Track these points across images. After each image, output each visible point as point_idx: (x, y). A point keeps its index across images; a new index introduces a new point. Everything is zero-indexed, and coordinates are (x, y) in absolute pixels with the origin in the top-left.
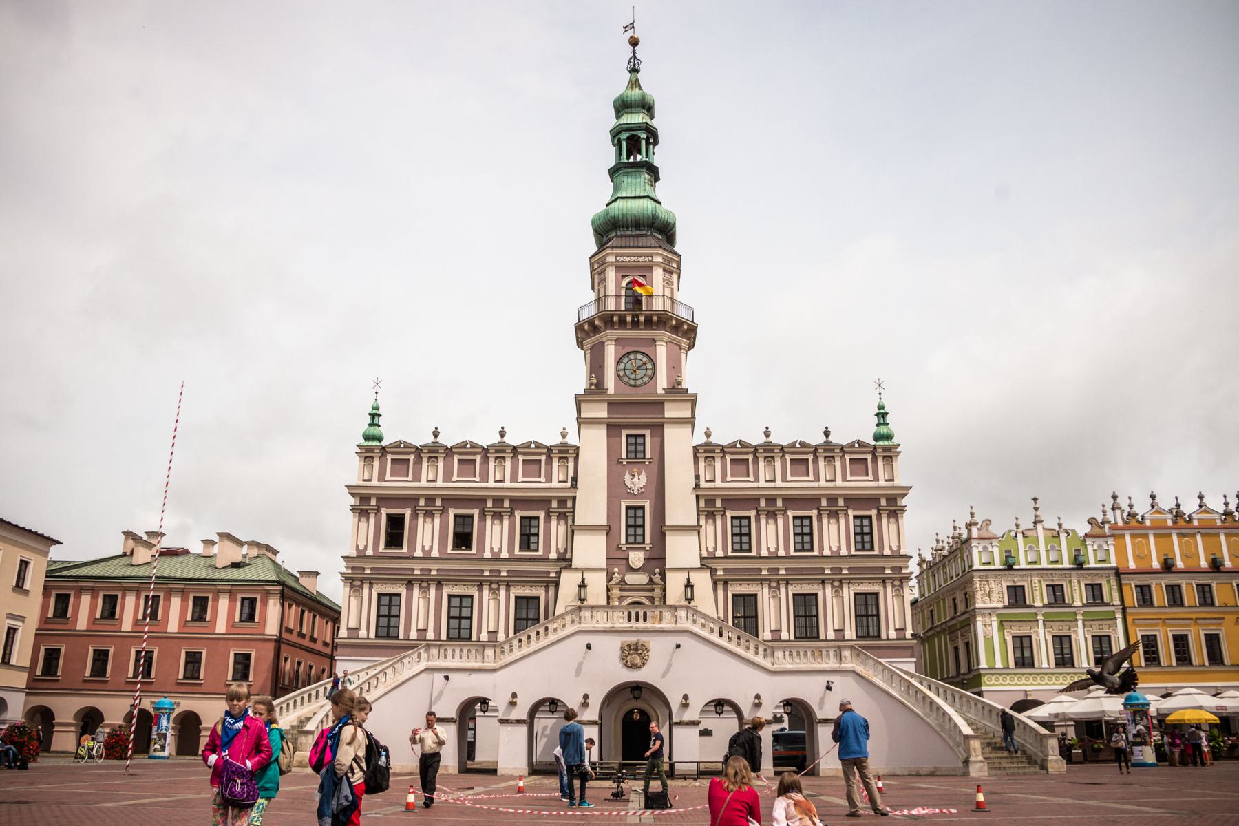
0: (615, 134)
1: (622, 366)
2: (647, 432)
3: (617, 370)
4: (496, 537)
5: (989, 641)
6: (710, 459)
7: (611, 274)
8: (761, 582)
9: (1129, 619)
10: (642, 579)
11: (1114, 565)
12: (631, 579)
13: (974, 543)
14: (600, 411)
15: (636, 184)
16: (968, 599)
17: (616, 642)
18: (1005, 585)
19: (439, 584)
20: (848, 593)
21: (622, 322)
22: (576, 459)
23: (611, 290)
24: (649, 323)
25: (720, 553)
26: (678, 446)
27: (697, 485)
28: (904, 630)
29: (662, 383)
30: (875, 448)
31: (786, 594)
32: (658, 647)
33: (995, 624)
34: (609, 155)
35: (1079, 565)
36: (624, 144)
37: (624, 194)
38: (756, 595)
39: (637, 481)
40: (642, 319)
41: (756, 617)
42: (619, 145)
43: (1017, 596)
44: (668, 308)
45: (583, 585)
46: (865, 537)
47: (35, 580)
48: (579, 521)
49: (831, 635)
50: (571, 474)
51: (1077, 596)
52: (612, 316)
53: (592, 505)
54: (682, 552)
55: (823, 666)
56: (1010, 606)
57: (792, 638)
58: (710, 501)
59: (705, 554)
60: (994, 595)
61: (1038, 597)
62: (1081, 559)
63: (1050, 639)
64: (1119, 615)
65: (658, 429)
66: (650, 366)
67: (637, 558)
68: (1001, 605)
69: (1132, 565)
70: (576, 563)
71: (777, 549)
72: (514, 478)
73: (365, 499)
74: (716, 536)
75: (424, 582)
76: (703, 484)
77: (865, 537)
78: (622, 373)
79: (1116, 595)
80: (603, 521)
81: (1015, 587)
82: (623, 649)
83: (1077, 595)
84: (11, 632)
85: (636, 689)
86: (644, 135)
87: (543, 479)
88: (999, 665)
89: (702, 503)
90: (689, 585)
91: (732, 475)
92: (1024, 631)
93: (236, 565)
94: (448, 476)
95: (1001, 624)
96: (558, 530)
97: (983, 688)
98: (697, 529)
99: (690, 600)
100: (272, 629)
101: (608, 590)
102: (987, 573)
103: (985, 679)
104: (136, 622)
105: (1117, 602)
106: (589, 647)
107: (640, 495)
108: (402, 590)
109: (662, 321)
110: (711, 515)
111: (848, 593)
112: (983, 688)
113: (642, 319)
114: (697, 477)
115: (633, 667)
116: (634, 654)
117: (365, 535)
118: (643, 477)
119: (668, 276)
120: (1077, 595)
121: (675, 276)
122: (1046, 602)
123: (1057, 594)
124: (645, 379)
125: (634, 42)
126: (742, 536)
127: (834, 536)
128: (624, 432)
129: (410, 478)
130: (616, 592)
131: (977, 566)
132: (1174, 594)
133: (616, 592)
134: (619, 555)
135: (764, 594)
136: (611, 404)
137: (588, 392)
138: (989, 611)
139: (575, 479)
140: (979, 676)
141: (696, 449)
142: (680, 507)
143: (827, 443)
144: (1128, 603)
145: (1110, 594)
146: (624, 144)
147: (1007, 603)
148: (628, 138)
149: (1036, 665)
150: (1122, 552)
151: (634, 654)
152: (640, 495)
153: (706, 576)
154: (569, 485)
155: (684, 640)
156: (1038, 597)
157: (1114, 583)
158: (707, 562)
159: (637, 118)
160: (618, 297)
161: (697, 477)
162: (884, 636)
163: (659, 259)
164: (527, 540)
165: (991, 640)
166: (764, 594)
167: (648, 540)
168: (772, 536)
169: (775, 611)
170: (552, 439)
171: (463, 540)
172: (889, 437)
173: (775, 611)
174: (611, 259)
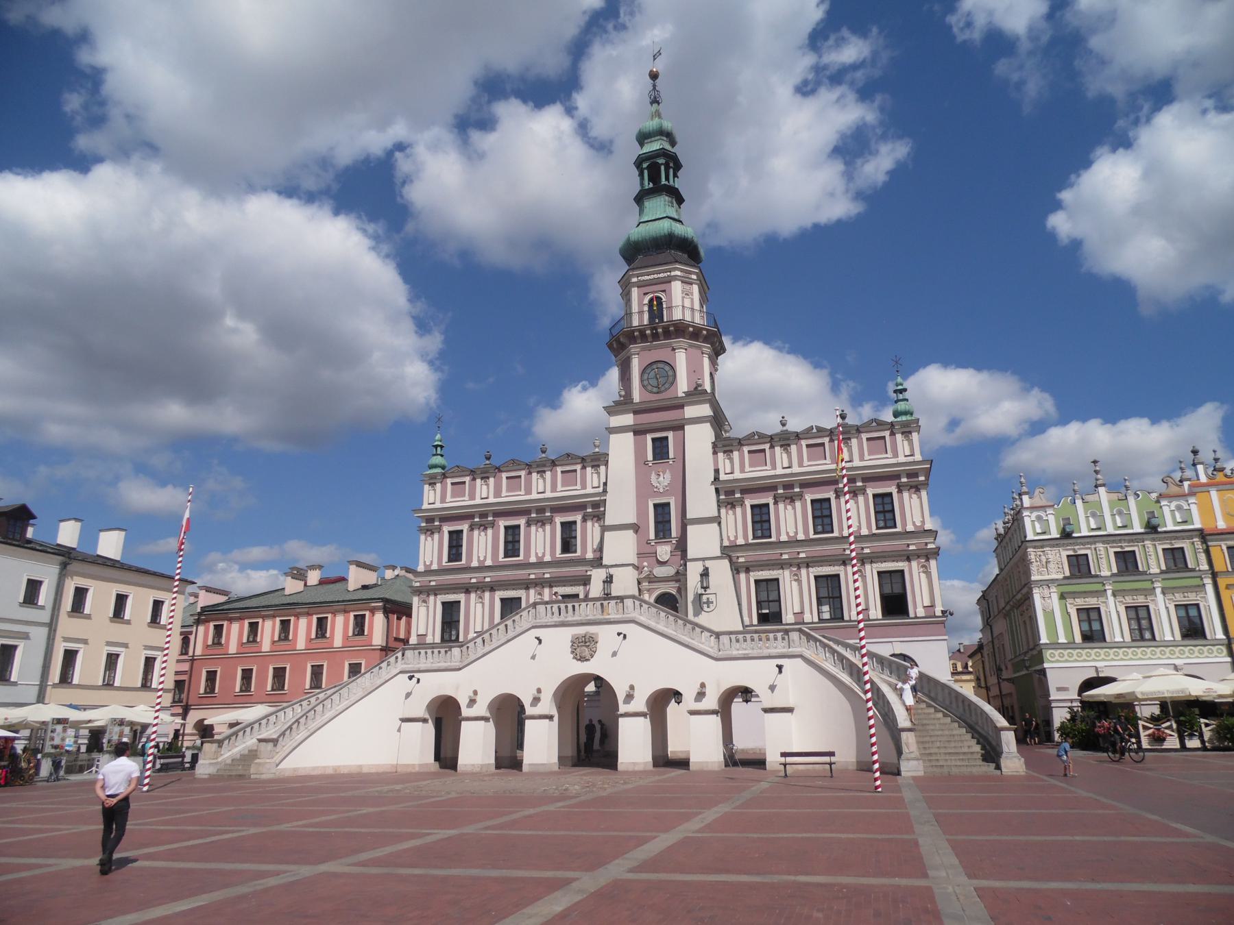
0: (638, 163)
1: (646, 376)
2: (670, 435)
3: (642, 381)
4: (541, 543)
5: (1050, 615)
6: (728, 452)
7: (635, 292)
8: (782, 565)
9: (1222, 582)
10: (669, 571)
11: (1198, 525)
12: (660, 572)
13: (1025, 513)
15: (659, 206)
16: (1028, 573)
17: (567, 634)
18: (1065, 554)
19: (492, 589)
20: (871, 571)
21: (643, 337)
22: (606, 464)
23: (635, 308)
24: (667, 334)
25: (741, 541)
27: (716, 479)
28: (933, 606)
29: (683, 385)
30: (892, 424)
31: (808, 577)
33: (1055, 597)
35: (1152, 528)
36: (646, 172)
37: (646, 219)
38: (777, 580)
39: (662, 480)
40: (660, 330)
41: (779, 601)
42: (641, 175)
43: (1080, 566)
44: (688, 318)
45: (609, 580)
48: (609, 520)
49: (921, 612)
50: (603, 480)
51: (1153, 562)
52: (633, 331)
53: (621, 507)
54: (703, 542)
55: (773, 651)
56: (1072, 576)
57: (816, 620)
58: (730, 492)
59: (726, 543)
60: (1051, 566)
61: (1105, 564)
62: (1154, 521)
64: (1208, 581)
65: (679, 427)
66: (670, 373)
67: (664, 551)
68: (1061, 576)
69: (1221, 525)
70: (605, 562)
71: (796, 533)
72: (554, 489)
73: (430, 520)
74: (737, 525)
75: (480, 588)
76: (722, 477)
78: (646, 383)
79: (1202, 557)
80: (631, 518)
81: (1077, 556)
82: (573, 642)
83: (1152, 558)
84: (150, 662)
85: (585, 678)
86: (661, 161)
87: (579, 487)
88: (1062, 640)
89: (722, 497)
90: (705, 574)
91: (751, 466)
92: (1091, 602)
93: (365, 587)
94: (498, 493)
95: (1062, 597)
96: (593, 529)
97: (1046, 665)
98: (717, 520)
99: (705, 588)
101: (639, 583)
102: (1041, 544)
103: (1047, 654)
104: (273, 642)
105: (1205, 567)
106: (540, 641)
107: (666, 493)
108: (461, 597)
109: (680, 330)
110: (732, 505)
111: (871, 571)
112: (1046, 665)
113: (660, 330)
114: (717, 471)
115: (582, 659)
116: (584, 647)
117: (431, 551)
118: (668, 475)
119: (687, 287)
120: (1152, 558)
121: (695, 288)
122: (1115, 570)
123: (1127, 561)
124: (667, 386)
125: (654, 76)
127: (854, 516)
128: (649, 437)
129: (467, 498)
130: (645, 584)
131: (1030, 536)
133: (645, 584)
134: (648, 549)
135: (785, 576)
136: (635, 413)
137: (617, 403)
138: (1048, 583)
139: (605, 484)
140: (1040, 653)
141: (715, 445)
142: (702, 500)
143: (844, 426)
144: (1219, 567)
145: (1195, 558)
146: (646, 172)
147: (1068, 574)
148: (648, 168)
149: (1108, 639)
150: (1207, 511)
151: (584, 647)
152: (666, 493)
153: (726, 562)
154: (601, 489)
156: (1105, 564)
157: (1199, 545)
158: (728, 551)
159: (654, 146)
160: (641, 312)
161: (717, 471)
162: (912, 614)
163: (678, 273)
165: (1052, 613)
166: (785, 576)
167: (674, 534)
168: (791, 521)
169: (798, 595)
171: (512, 547)
172: (906, 413)
173: (798, 595)
174: (634, 280)
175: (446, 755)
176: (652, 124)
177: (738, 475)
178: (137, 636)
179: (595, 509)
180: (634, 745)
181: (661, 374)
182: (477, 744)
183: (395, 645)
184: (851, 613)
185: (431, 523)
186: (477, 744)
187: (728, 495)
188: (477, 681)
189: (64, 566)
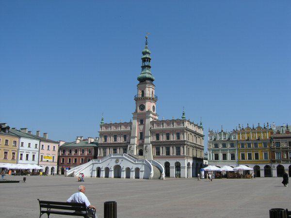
0: (142, 59)
14: (136, 116)
26: (148, 121)
32: (120, 160)
34: (141, 64)
43: (216, 146)
46: (178, 137)
47: (57, 149)
54: (148, 140)
61: (221, 146)
63: (222, 155)
77: (178, 137)
93: (91, 143)
100: (93, 154)
126: (158, 138)
132: (249, 145)
142: (148, 133)
151: (117, 161)
155: (124, 160)
156: (221, 146)
164: (125, 140)
168: (163, 138)
170: (128, 121)
175: (98, 175)
176: (145, 50)
177: (154, 128)
178: (51, 152)
179: (129, 133)
180: (124, 174)
181: (142, 107)
182: (103, 174)
183: (95, 157)
184: (171, 154)
185: (101, 134)
186: (103, 174)
187: (152, 132)
188: (103, 166)
189: (40, 141)
